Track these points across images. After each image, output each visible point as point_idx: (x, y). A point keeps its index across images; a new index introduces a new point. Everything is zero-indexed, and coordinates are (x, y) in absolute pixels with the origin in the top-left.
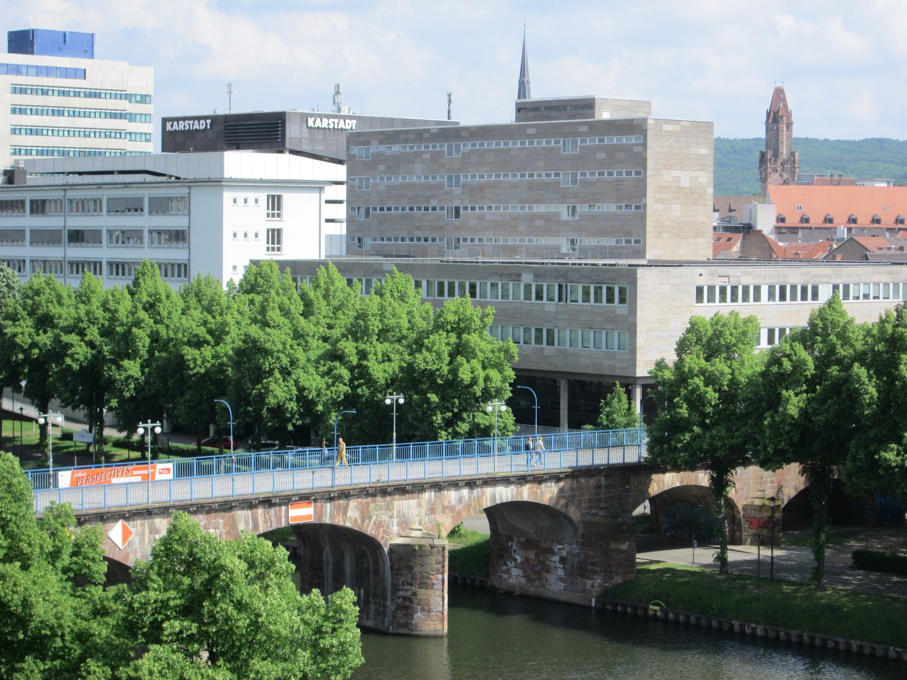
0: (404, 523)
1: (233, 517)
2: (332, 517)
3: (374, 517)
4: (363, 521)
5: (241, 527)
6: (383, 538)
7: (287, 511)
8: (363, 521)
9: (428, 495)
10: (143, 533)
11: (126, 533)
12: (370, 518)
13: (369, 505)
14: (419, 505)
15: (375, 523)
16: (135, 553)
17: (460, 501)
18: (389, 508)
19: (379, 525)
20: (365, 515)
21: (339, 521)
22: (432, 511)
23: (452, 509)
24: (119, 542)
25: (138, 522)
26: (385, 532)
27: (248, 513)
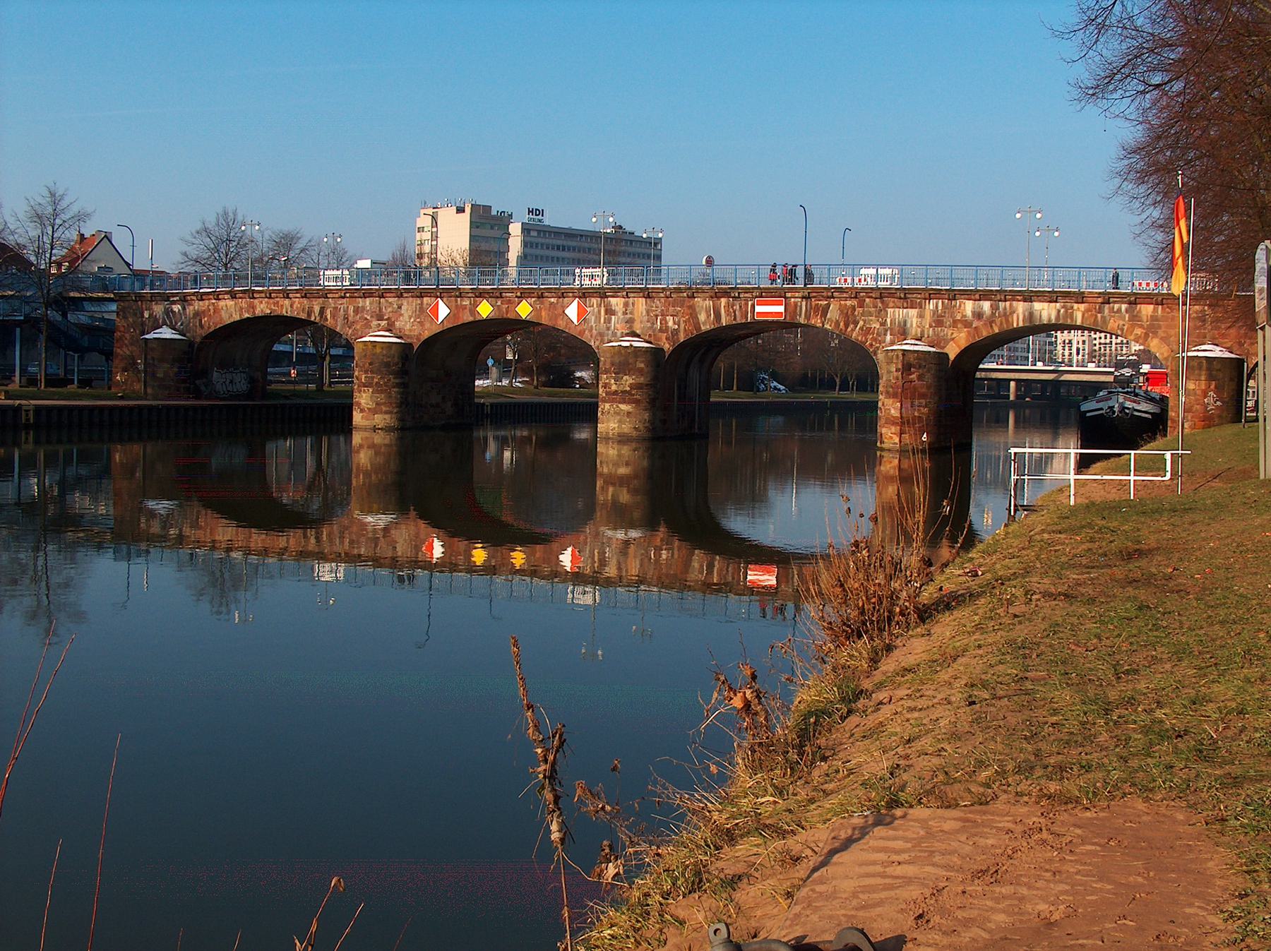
0: (902, 332)
1: (692, 307)
2: (808, 317)
3: (861, 323)
4: (847, 326)
5: (702, 317)
6: (871, 345)
7: (753, 306)
8: (847, 326)
9: (931, 305)
10: (599, 312)
11: (581, 312)
12: (856, 323)
13: (854, 308)
14: (921, 316)
15: (861, 329)
16: (591, 330)
17: (978, 315)
18: (881, 313)
19: (868, 331)
20: (849, 317)
21: (816, 321)
22: (938, 322)
23: (967, 324)
24: (575, 321)
25: (594, 301)
26: (875, 339)
27: (709, 303)
